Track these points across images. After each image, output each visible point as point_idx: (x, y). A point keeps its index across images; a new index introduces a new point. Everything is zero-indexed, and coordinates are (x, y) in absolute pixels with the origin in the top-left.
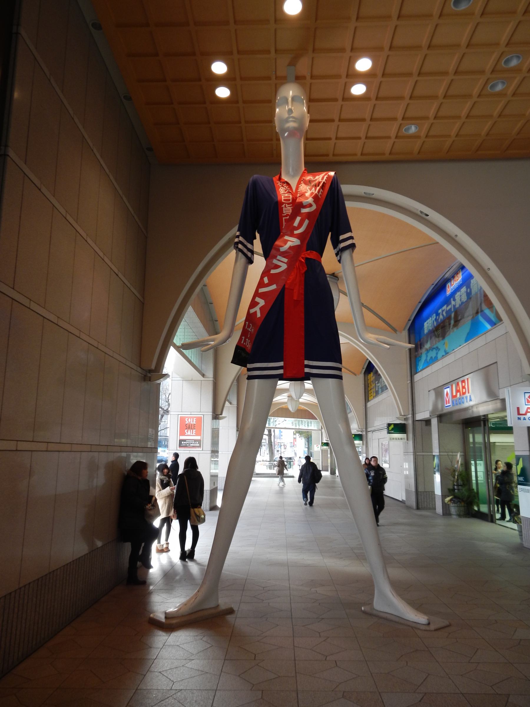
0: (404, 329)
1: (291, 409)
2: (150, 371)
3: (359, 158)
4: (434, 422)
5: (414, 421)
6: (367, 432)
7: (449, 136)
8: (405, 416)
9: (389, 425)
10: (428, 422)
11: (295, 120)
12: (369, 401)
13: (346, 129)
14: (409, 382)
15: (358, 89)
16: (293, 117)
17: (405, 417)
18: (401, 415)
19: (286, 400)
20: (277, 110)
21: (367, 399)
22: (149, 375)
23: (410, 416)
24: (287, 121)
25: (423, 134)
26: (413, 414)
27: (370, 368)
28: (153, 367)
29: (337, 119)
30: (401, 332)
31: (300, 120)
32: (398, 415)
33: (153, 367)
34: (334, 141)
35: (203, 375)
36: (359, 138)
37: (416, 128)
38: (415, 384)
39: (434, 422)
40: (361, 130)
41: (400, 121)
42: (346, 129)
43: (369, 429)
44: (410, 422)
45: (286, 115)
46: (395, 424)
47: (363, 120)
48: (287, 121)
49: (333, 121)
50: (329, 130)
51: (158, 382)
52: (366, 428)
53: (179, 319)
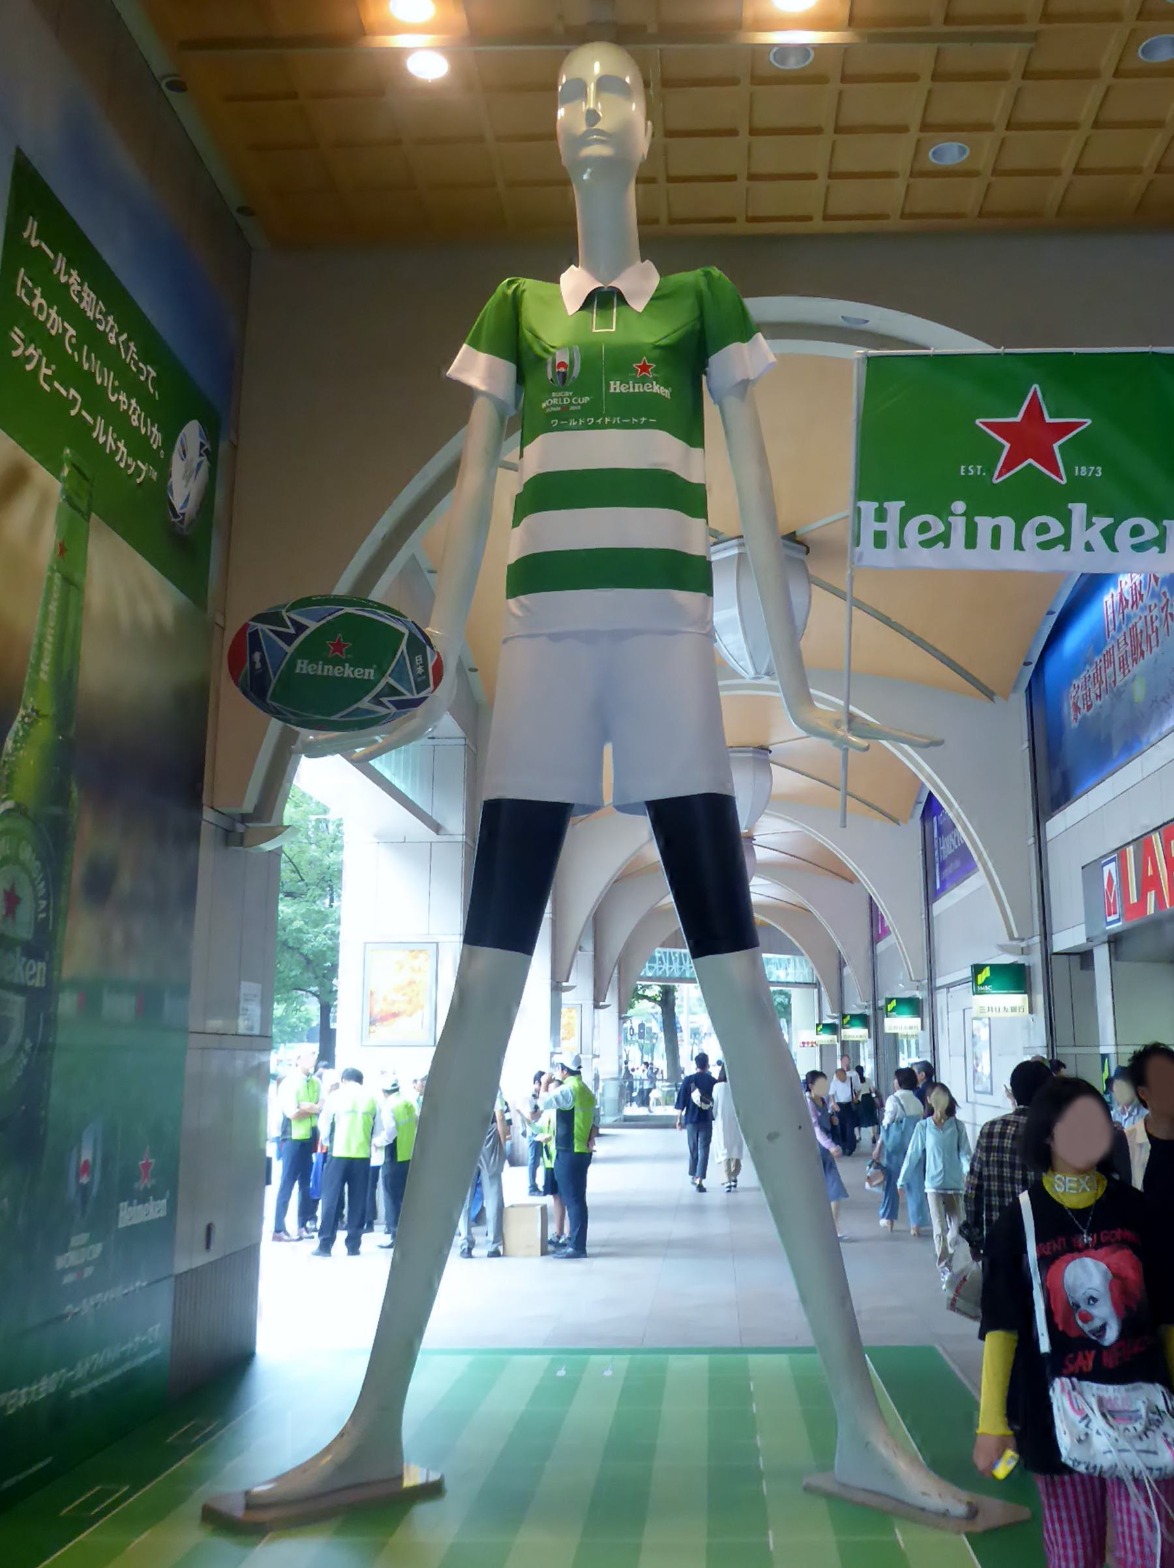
0: (1015, 688)
3: (817, 225)
4: (1102, 956)
5: (1048, 956)
6: (932, 990)
7: (1056, 172)
8: (1023, 940)
9: (977, 969)
10: (1085, 958)
11: (607, 137)
13: (771, 155)
14: (1031, 841)
16: (600, 132)
17: (1023, 944)
18: (1011, 937)
20: (561, 113)
23: (1037, 939)
24: (583, 140)
25: (984, 162)
26: (1046, 936)
27: (931, 807)
29: (744, 129)
30: (1006, 697)
31: (620, 138)
32: (1005, 940)
34: (743, 182)
36: (813, 176)
37: (962, 151)
38: (1049, 844)
39: (1102, 956)
40: (813, 154)
43: (939, 982)
44: (1035, 960)
45: (583, 128)
46: (994, 967)
47: (817, 131)
48: (583, 140)
49: (733, 133)
50: (726, 156)
52: (931, 979)
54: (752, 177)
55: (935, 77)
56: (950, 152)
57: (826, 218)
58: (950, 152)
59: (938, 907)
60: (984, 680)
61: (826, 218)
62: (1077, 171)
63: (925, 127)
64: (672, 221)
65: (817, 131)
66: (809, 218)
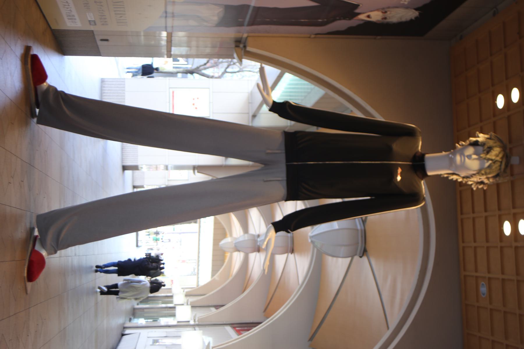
1: (223, 242)
2: (245, 47)
12: (234, 328)
15: (507, 228)
19: (235, 235)
21: (233, 325)
22: (241, 46)
28: (249, 49)
29: (487, 214)
33: (249, 49)
35: (254, 116)
37: (484, 294)
41: (488, 276)
42: (480, 223)
49: (486, 211)
51: (235, 55)
52: (198, 325)
53: (298, 73)
54: (474, 219)
55: (503, 280)
56: (483, 289)
57: (464, 248)
58: (483, 289)
59: (229, 329)
60: (317, 336)
61: (464, 248)
62: (480, 338)
63: (490, 279)
64: (461, 192)
65: (487, 241)
66: (463, 242)
